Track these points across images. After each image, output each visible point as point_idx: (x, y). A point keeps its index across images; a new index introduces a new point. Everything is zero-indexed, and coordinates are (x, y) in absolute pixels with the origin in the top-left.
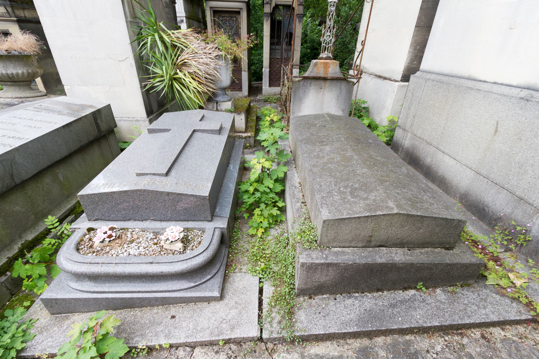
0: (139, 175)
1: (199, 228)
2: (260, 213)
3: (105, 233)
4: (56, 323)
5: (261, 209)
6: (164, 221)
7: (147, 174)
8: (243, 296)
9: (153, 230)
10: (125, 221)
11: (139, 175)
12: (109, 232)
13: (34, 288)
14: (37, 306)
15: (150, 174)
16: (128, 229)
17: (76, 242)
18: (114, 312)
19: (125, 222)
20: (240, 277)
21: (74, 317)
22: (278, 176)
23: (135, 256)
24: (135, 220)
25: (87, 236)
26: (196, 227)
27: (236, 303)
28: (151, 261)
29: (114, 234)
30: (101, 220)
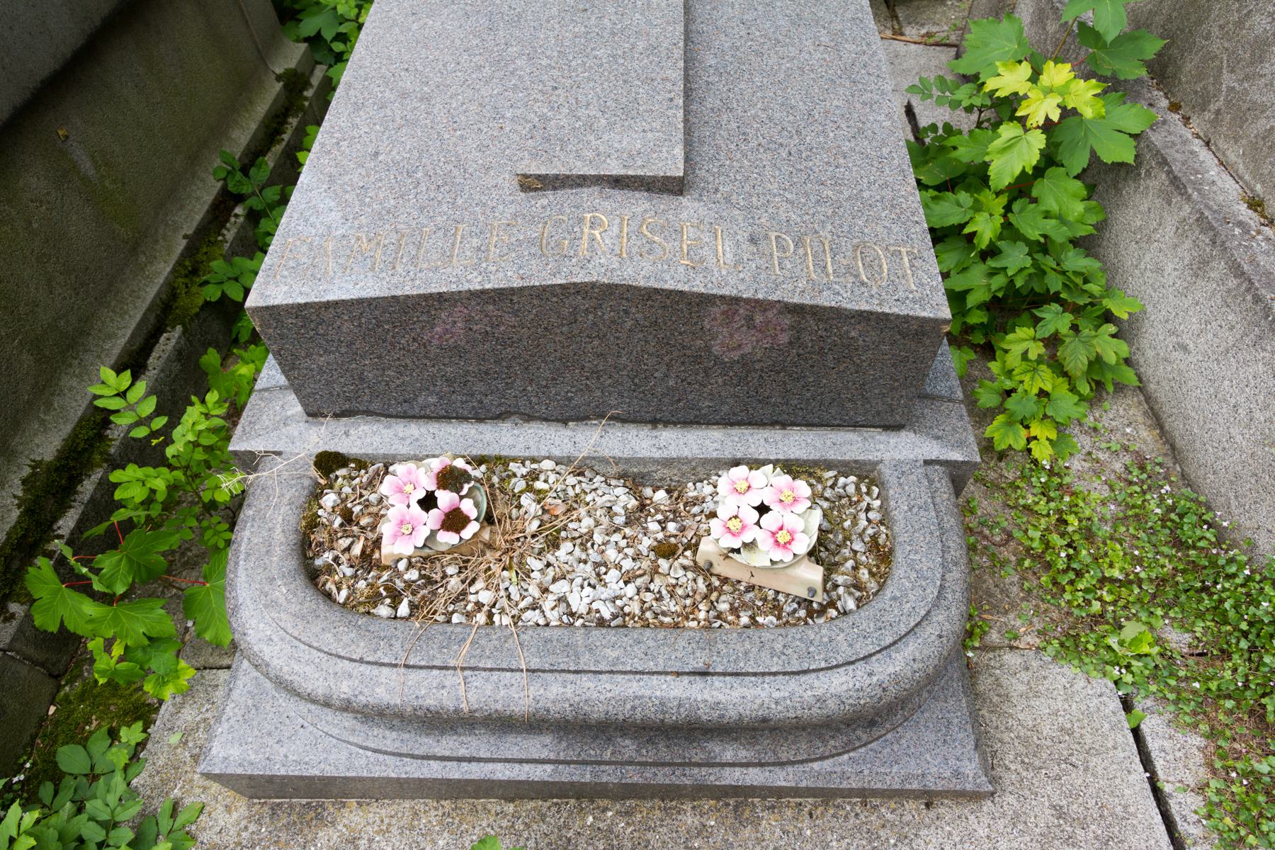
0: (532, 184)
1: (845, 464)
2: (1036, 350)
3: (428, 502)
4: (283, 836)
5: (1046, 331)
6: (667, 423)
7: (581, 181)
8: (1077, 778)
9: (621, 467)
10: (480, 420)
11: (532, 184)
12: (445, 499)
13: (143, 678)
14: (174, 739)
15: (599, 180)
16: (504, 461)
17: (293, 538)
18: (510, 808)
19: (482, 427)
20: (1024, 676)
21: (345, 812)
22: (1094, 157)
23: (601, 623)
24: (529, 418)
25: (329, 499)
26: (832, 455)
27: (1060, 812)
28: (700, 666)
29: (467, 507)
30: (368, 413)
